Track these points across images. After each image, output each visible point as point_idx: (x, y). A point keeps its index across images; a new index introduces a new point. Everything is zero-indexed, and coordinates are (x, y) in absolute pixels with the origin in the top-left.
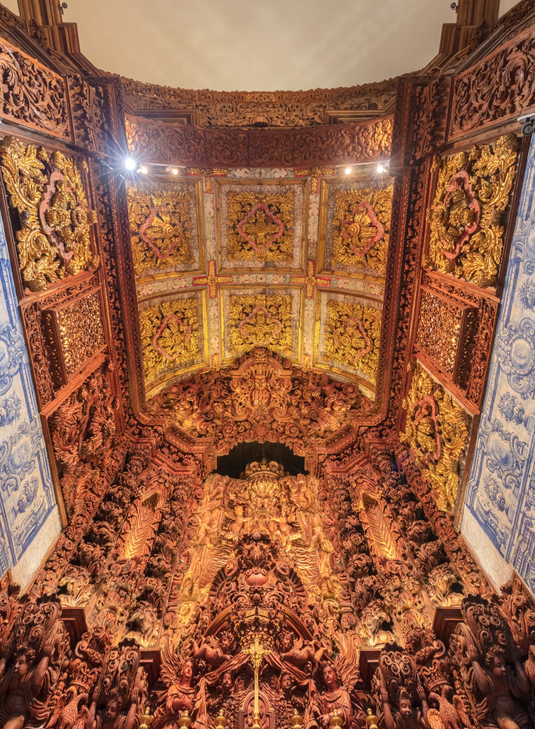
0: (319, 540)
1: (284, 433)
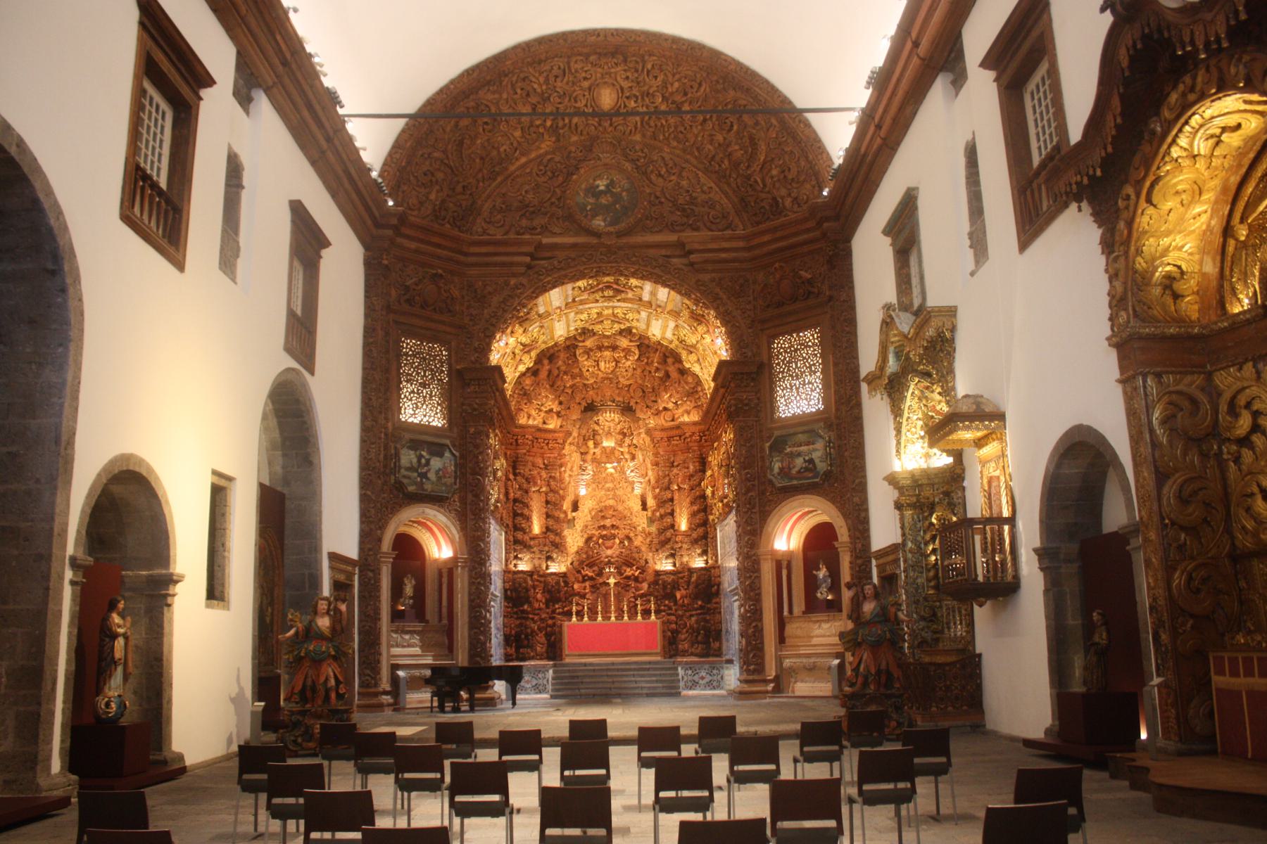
0: (649, 481)
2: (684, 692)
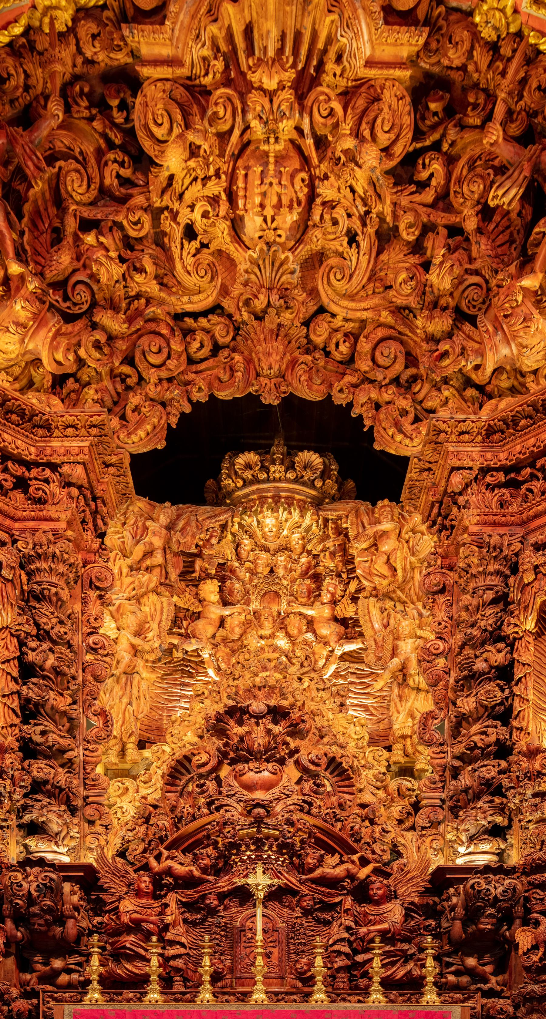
1: (350, 360)
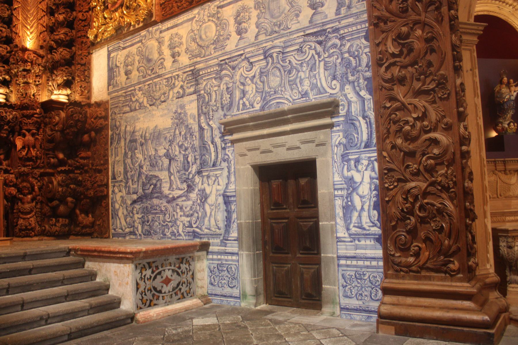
2: (141, 315)
